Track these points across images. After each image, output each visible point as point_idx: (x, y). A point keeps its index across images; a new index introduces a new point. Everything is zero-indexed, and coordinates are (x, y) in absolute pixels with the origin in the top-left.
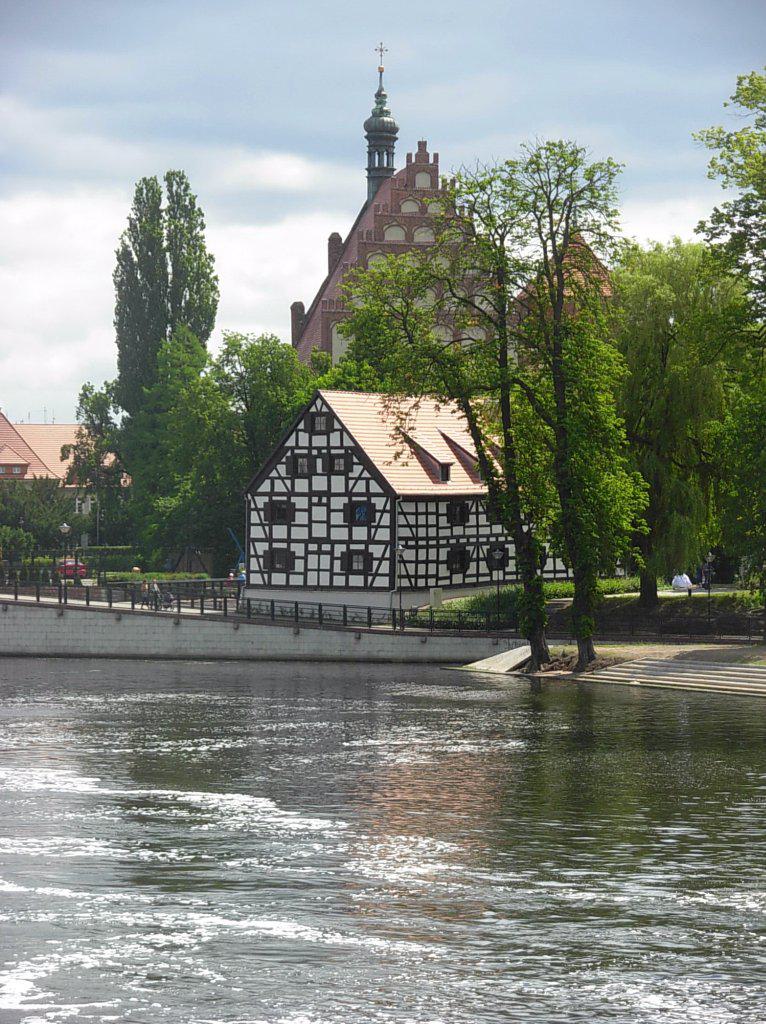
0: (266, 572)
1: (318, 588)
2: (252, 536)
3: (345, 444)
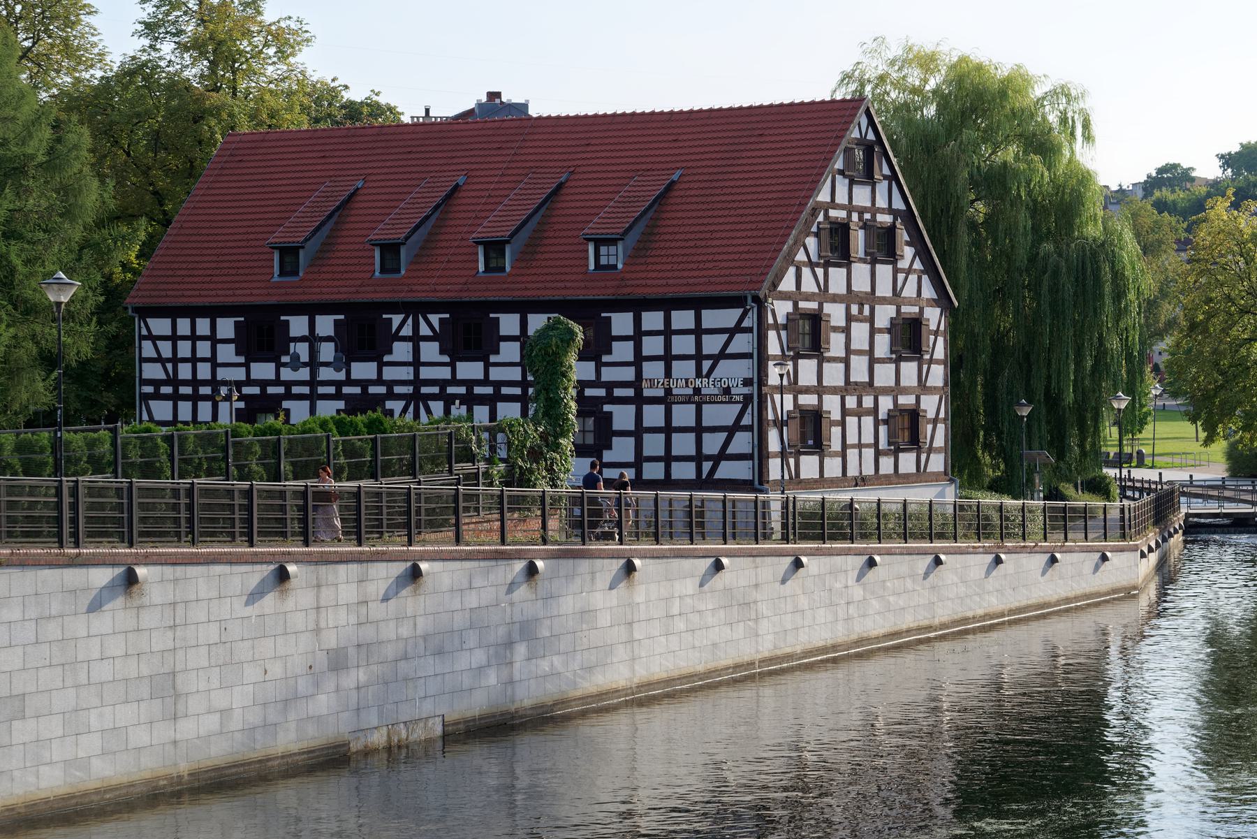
1: (861, 481)
3: (894, 206)
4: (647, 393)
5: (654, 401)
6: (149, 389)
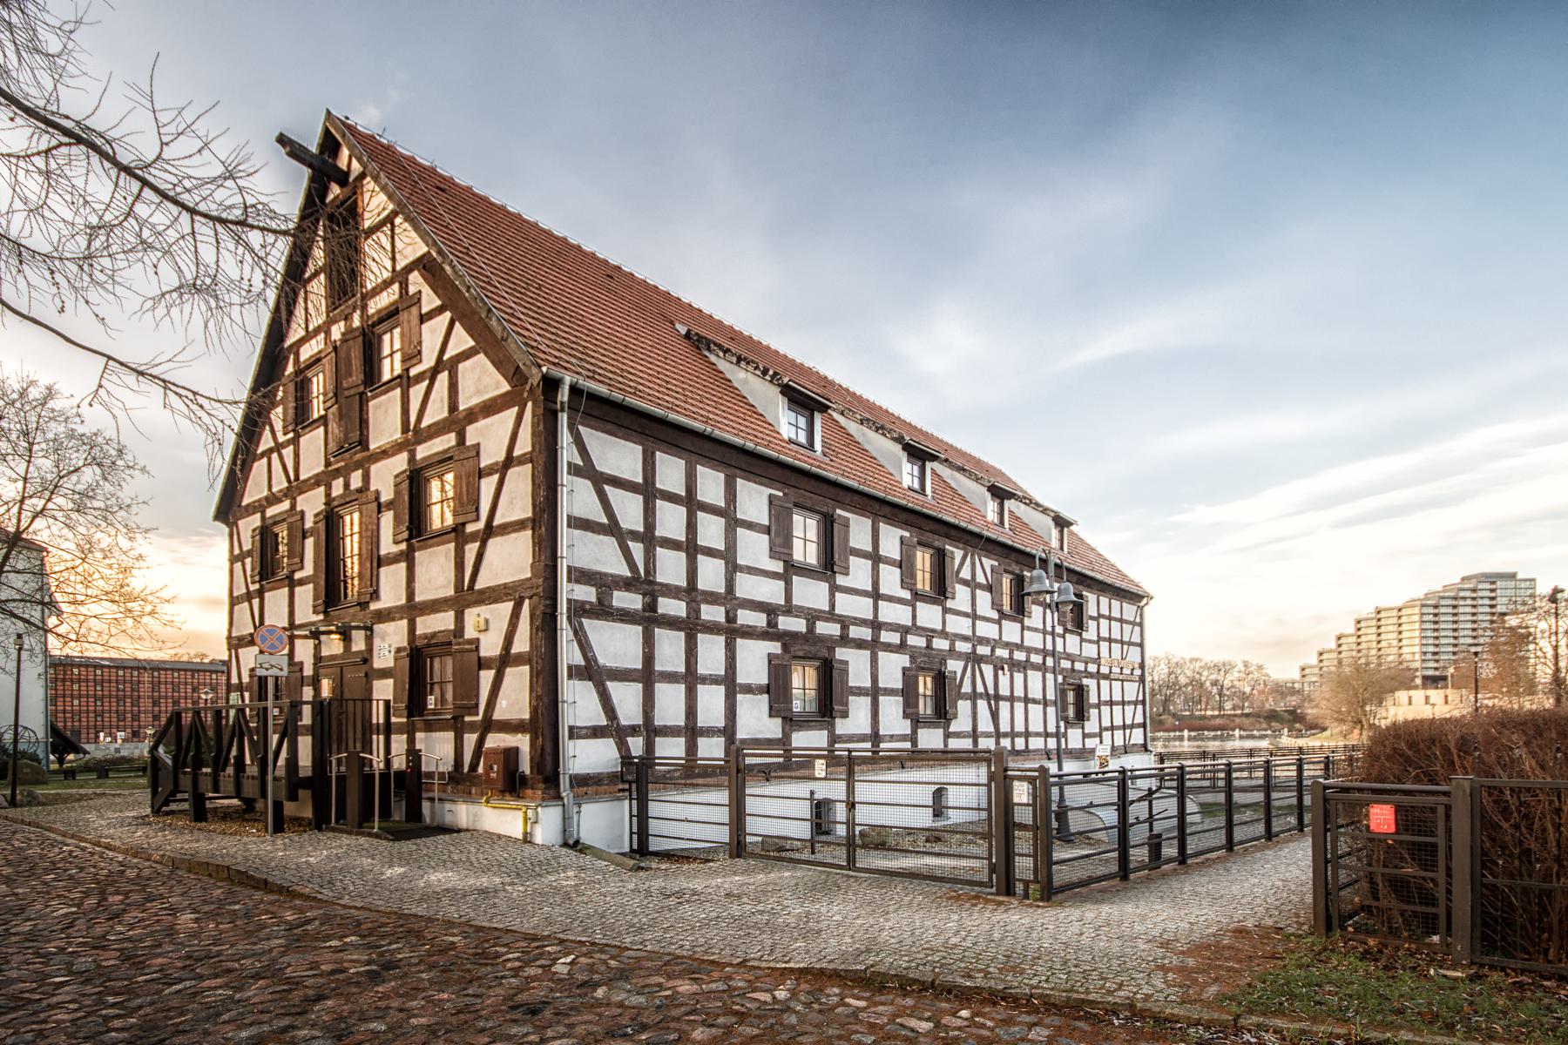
6: (587, 593)
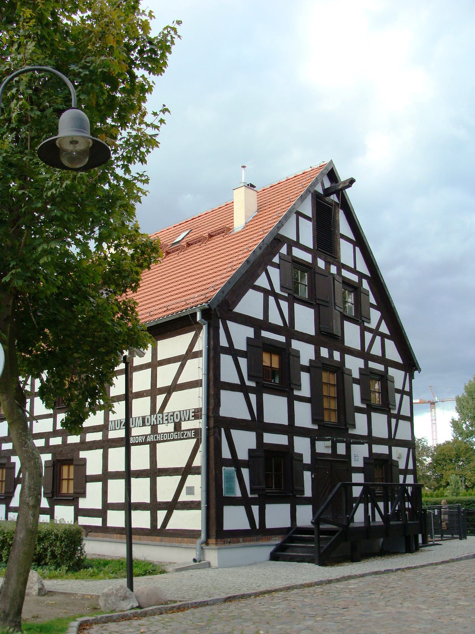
0: (254, 502)
2: (224, 412)
4: (112, 435)
5: (116, 443)
